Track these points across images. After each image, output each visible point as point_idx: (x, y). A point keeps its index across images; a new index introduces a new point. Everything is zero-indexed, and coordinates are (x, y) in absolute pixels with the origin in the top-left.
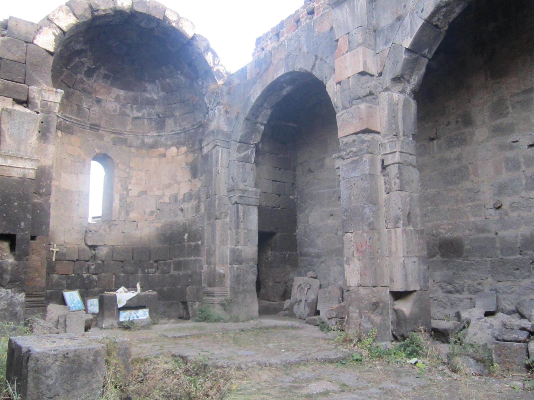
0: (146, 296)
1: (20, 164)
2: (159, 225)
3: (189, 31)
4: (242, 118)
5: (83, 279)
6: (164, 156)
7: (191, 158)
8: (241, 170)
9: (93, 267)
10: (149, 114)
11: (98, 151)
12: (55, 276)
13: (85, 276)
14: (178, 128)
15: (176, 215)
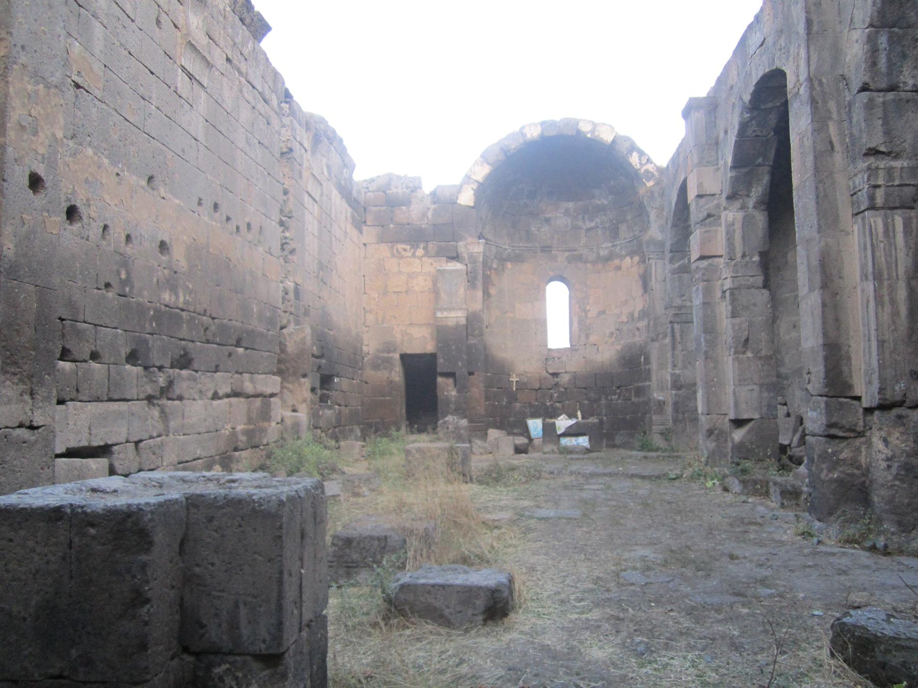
0: (585, 424)
1: (453, 314)
2: (619, 347)
3: (607, 137)
4: (669, 225)
5: (547, 408)
6: (619, 268)
7: (641, 271)
8: (677, 284)
9: (556, 395)
10: (602, 223)
11: (551, 274)
12: (518, 405)
13: (548, 404)
14: (632, 234)
15: (634, 335)
